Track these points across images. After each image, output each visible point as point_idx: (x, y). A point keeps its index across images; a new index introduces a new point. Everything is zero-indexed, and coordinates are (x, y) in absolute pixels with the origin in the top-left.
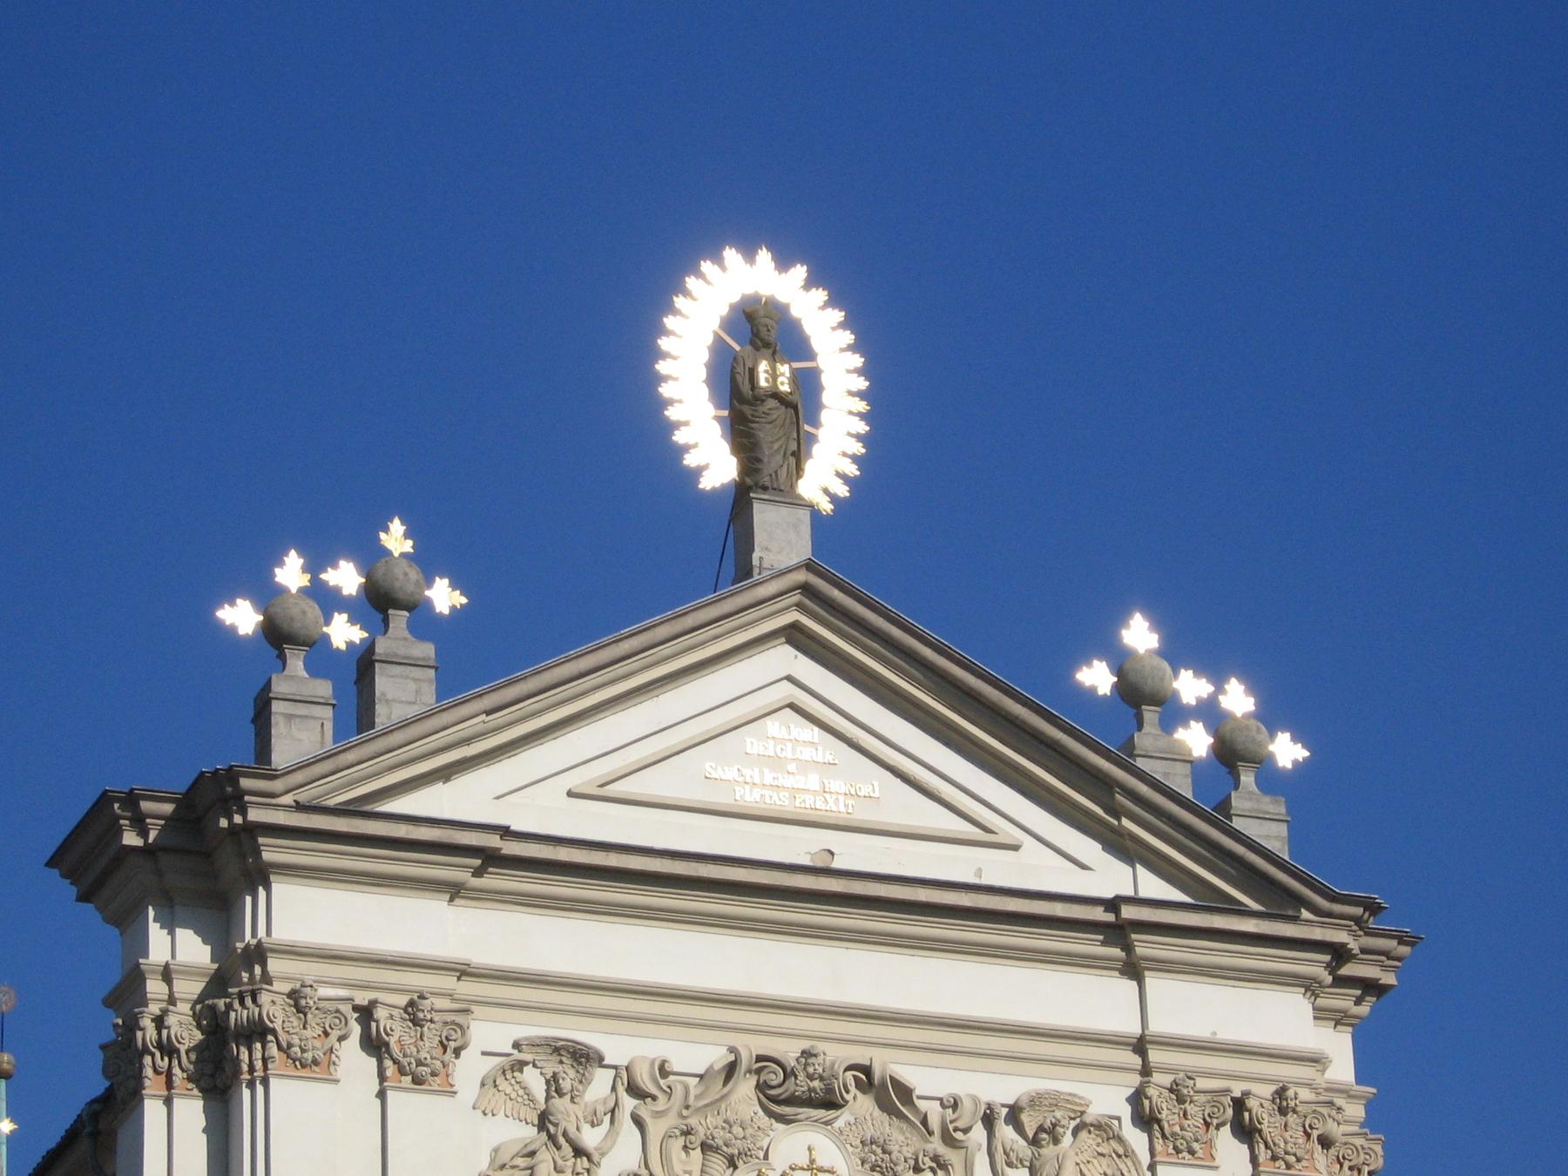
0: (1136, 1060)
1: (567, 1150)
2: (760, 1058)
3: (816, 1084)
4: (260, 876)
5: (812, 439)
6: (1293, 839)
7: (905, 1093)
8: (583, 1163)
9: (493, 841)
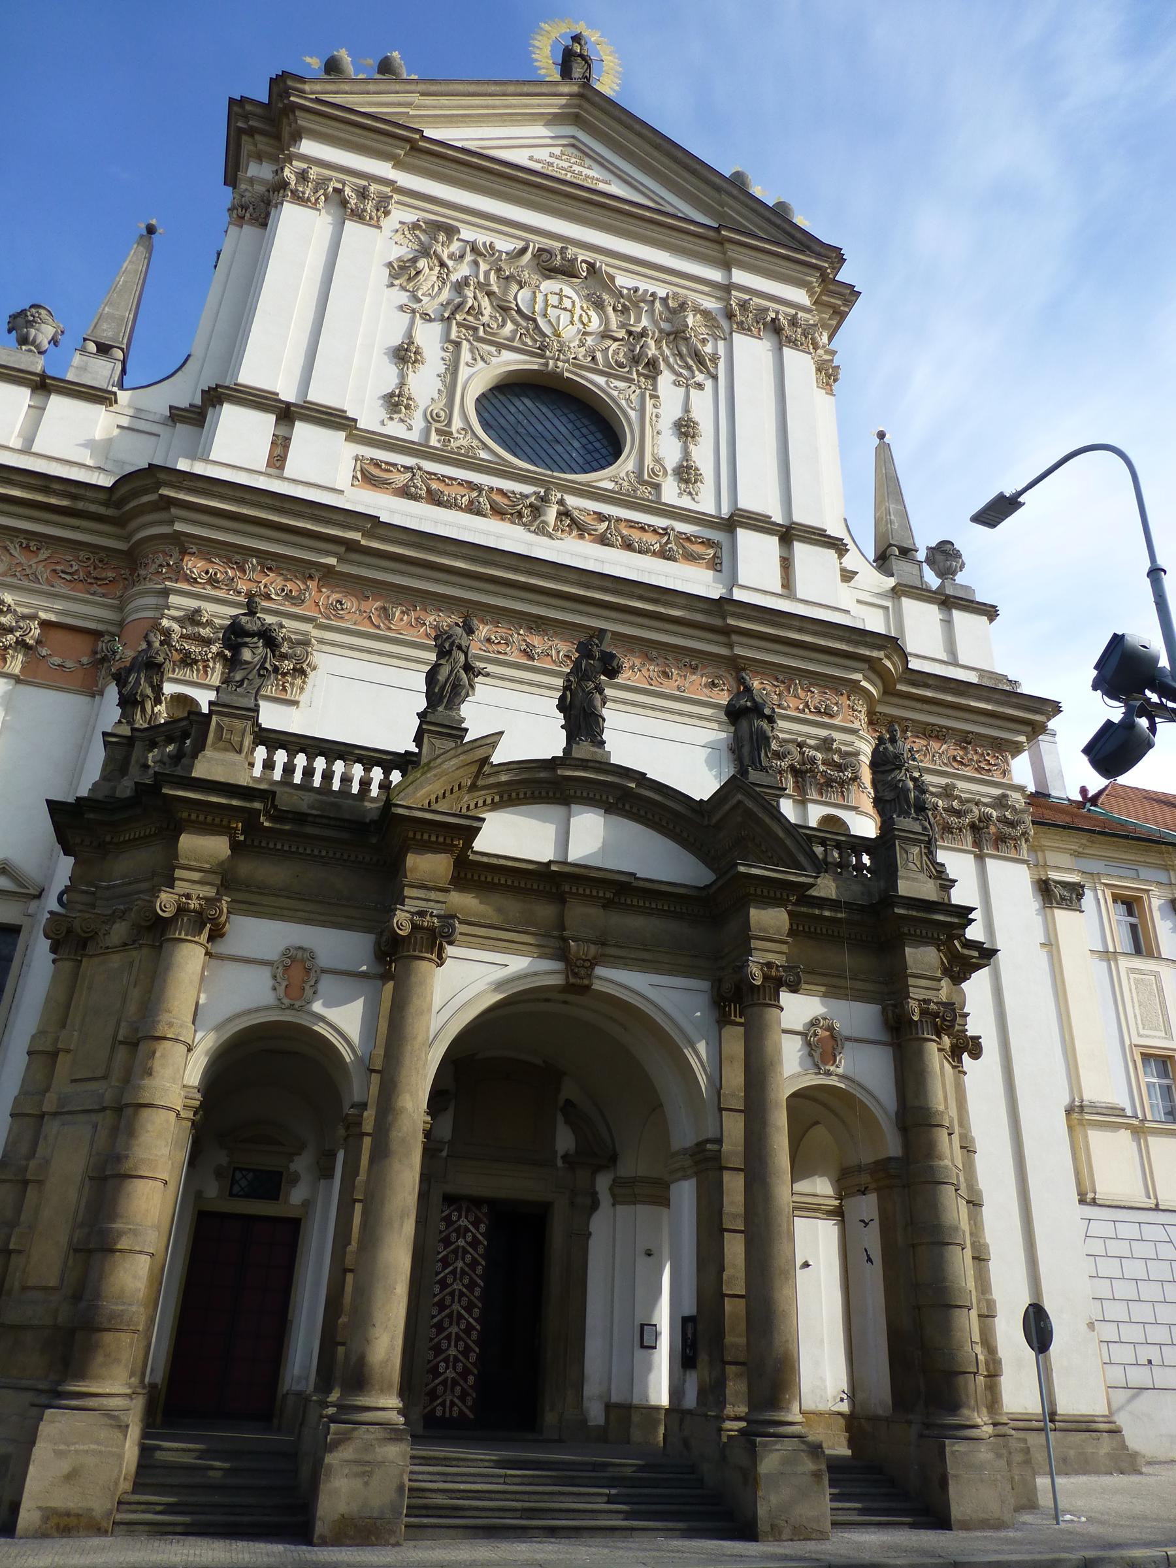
4: (297, 137)
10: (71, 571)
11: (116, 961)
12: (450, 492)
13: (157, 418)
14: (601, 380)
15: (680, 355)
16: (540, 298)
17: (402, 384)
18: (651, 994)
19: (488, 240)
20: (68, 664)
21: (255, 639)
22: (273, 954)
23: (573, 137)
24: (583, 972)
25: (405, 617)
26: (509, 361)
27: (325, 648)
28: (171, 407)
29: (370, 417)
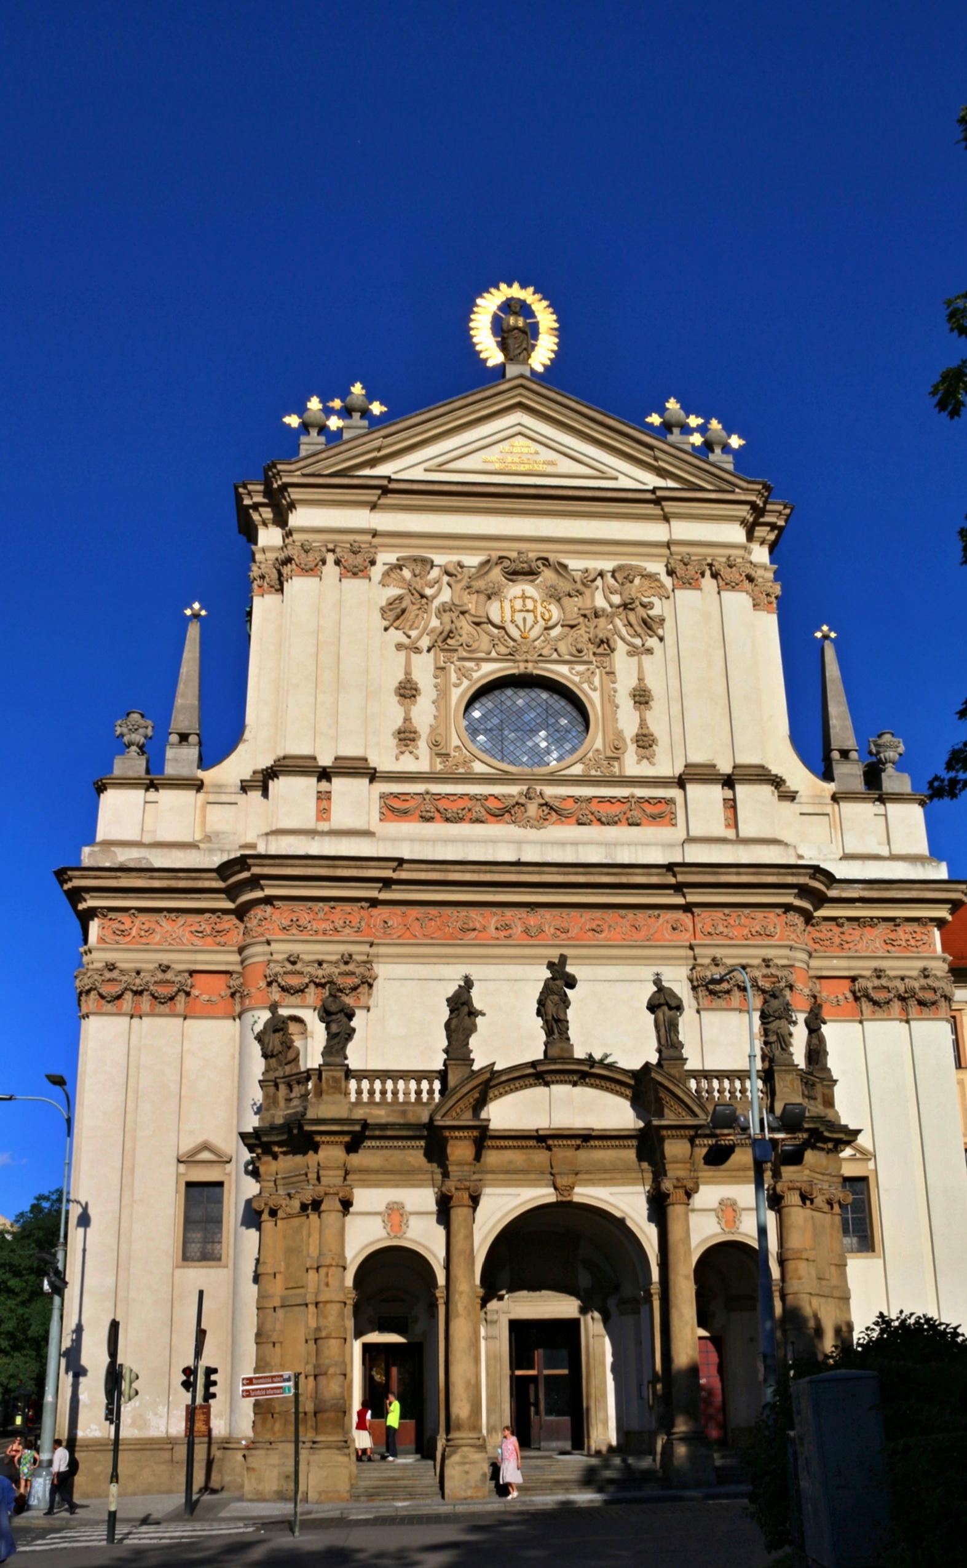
0: (666, 551)
1: (417, 595)
2: (500, 558)
3: (525, 565)
5: (534, 346)
6: (735, 468)
7: (565, 567)
8: (424, 601)
9: (385, 482)
10: (201, 929)
11: (296, 1222)
12: (453, 808)
13: (233, 790)
14: (564, 669)
15: (631, 626)
16: (507, 605)
17: (407, 719)
18: (611, 1199)
19: (455, 558)
20: (213, 999)
21: (339, 1015)
22: (382, 1208)
23: (519, 424)
24: (566, 1193)
25: (433, 923)
26: (489, 670)
27: (380, 960)
28: (242, 781)
29: (383, 760)
